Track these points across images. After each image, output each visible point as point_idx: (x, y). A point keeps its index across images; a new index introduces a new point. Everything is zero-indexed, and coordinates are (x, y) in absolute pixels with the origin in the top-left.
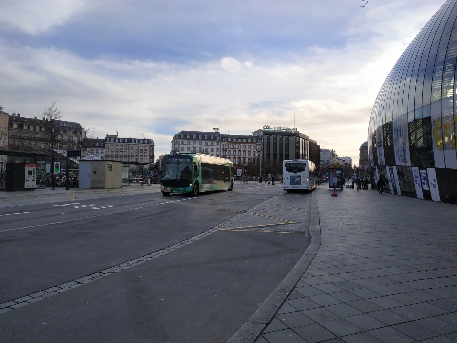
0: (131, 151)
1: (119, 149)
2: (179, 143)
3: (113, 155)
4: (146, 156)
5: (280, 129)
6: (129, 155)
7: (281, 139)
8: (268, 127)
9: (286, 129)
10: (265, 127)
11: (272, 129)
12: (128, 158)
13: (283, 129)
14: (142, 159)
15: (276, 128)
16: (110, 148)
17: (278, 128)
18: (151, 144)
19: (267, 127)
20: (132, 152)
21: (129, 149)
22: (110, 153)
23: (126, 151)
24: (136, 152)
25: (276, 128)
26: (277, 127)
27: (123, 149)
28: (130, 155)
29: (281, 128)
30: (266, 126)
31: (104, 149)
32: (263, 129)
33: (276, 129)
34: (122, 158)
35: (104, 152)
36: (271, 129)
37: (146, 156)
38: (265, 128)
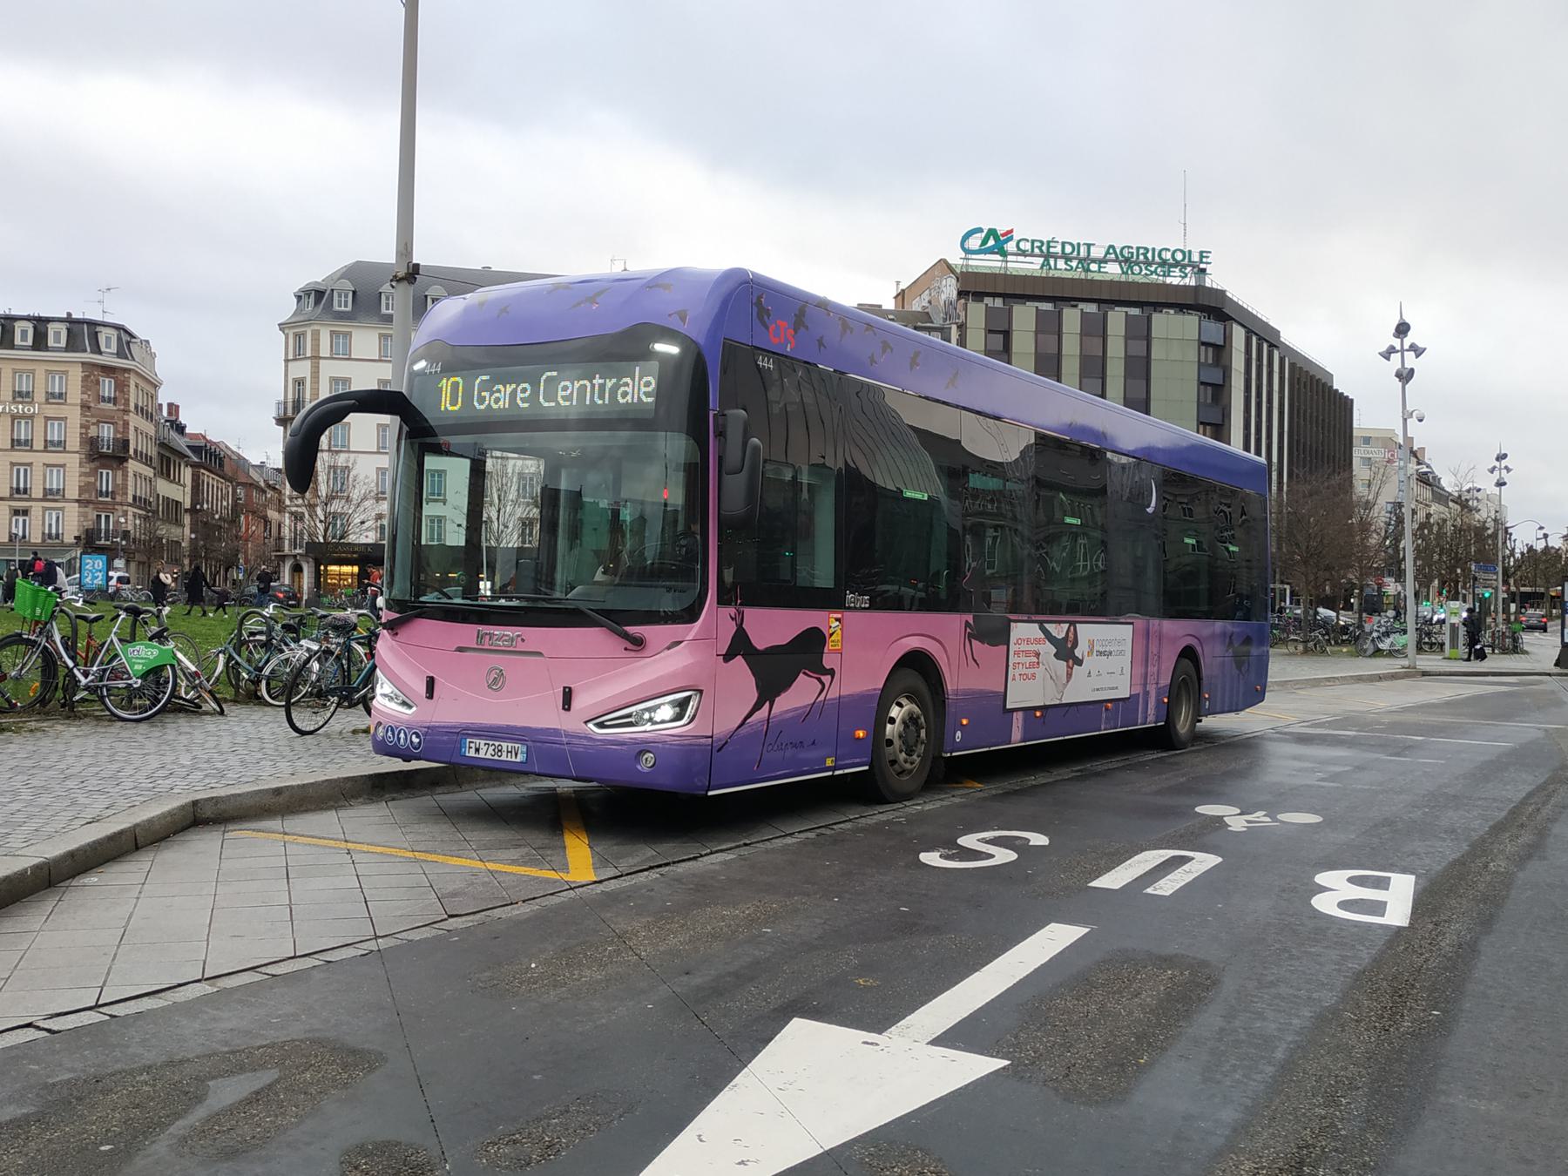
2: (316, 347)
4: (61, 445)
5: (1083, 254)
7: (1095, 330)
8: (997, 241)
9: (1127, 260)
10: (974, 243)
11: (1024, 253)
13: (1104, 261)
14: (30, 464)
15: (1058, 249)
17: (1068, 249)
18: (100, 353)
19: (991, 242)
25: (1058, 249)
26: (1063, 244)
29: (1089, 246)
30: (980, 230)
32: (963, 255)
33: (1056, 257)
36: (1021, 258)
37: (61, 445)
38: (977, 248)
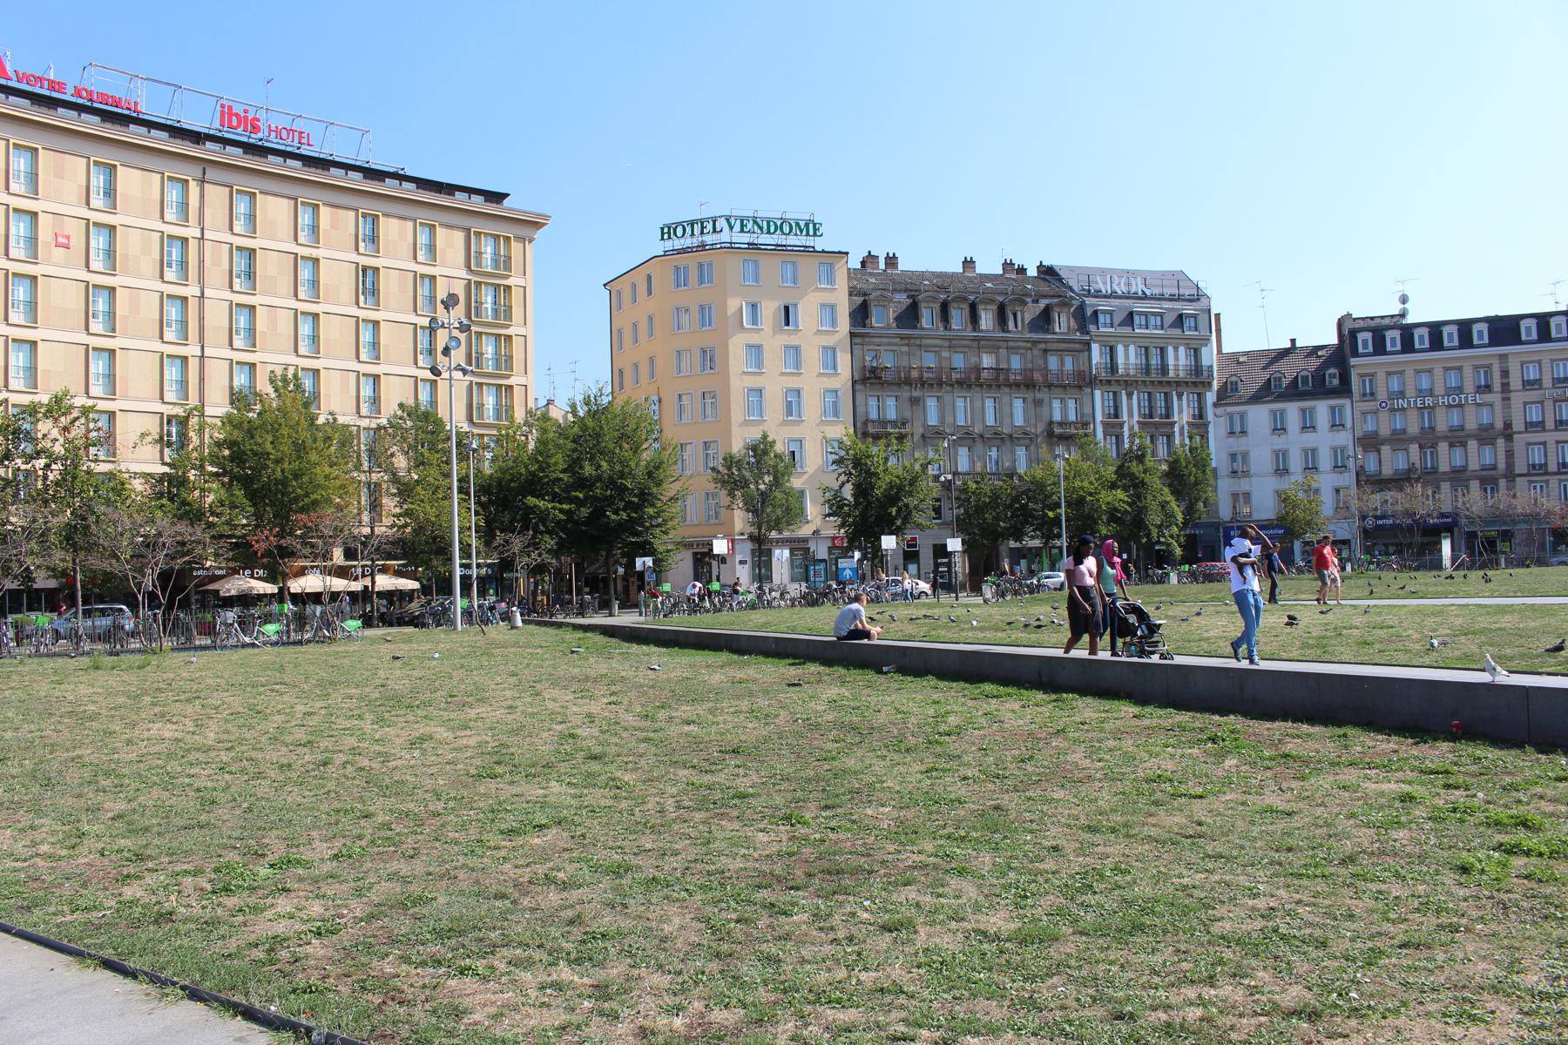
0: (1517, 399)
1: (1439, 390)
3: (1404, 431)
6: (1508, 425)
12: (1501, 442)
16: (1382, 394)
20: (1525, 404)
21: (1505, 387)
22: (1385, 425)
23: (1488, 398)
24: (1555, 401)
27: (1469, 386)
28: (1518, 425)
31: (1347, 402)
34: (1464, 444)
35: (1349, 424)
